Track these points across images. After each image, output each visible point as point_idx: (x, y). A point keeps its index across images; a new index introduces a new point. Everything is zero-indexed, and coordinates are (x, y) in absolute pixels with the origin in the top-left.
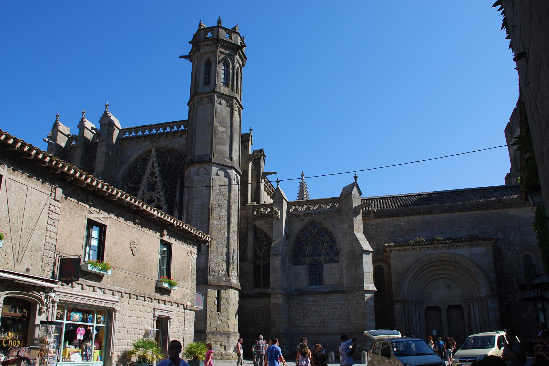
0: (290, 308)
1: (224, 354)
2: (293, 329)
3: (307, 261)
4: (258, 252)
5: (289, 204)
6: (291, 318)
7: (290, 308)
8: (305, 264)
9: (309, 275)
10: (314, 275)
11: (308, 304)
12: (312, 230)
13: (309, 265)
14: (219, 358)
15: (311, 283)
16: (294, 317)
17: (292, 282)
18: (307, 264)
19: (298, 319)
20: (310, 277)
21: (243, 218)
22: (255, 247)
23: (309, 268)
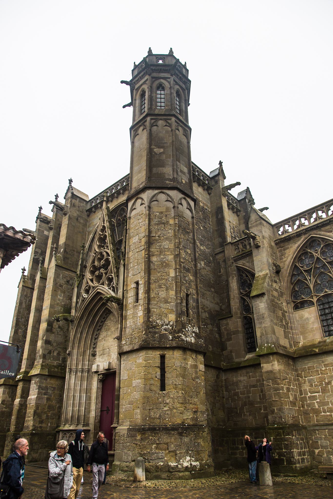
0: (300, 379)
1: (173, 468)
2: (311, 415)
3: (315, 300)
4: (246, 302)
5: (275, 228)
6: (303, 396)
7: (300, 379)
8: (312, 303)
9: (322, 321)
10: (330, 320)
11: (328, 368)
12: (313, 253)
13: (319, 305)
14: (164, 475)
15: (327, 333)
16: (309, 394)
17: (297, 336)
18: (315, 304)
19: (316, 396)
20: (325, 324)
21: (223, 262)
22: (241, 296)
23: (320, 310)
